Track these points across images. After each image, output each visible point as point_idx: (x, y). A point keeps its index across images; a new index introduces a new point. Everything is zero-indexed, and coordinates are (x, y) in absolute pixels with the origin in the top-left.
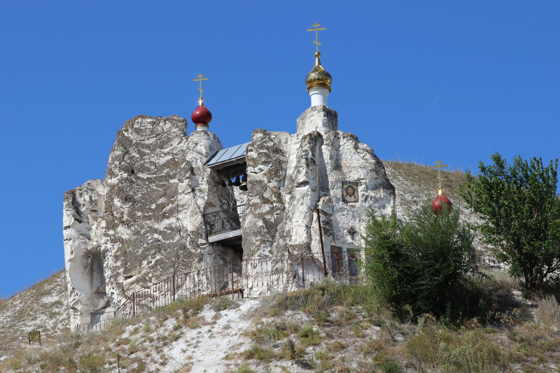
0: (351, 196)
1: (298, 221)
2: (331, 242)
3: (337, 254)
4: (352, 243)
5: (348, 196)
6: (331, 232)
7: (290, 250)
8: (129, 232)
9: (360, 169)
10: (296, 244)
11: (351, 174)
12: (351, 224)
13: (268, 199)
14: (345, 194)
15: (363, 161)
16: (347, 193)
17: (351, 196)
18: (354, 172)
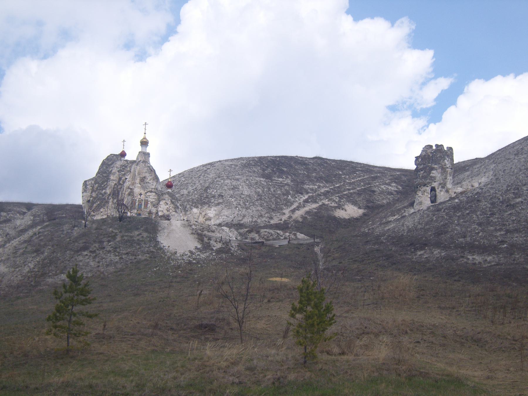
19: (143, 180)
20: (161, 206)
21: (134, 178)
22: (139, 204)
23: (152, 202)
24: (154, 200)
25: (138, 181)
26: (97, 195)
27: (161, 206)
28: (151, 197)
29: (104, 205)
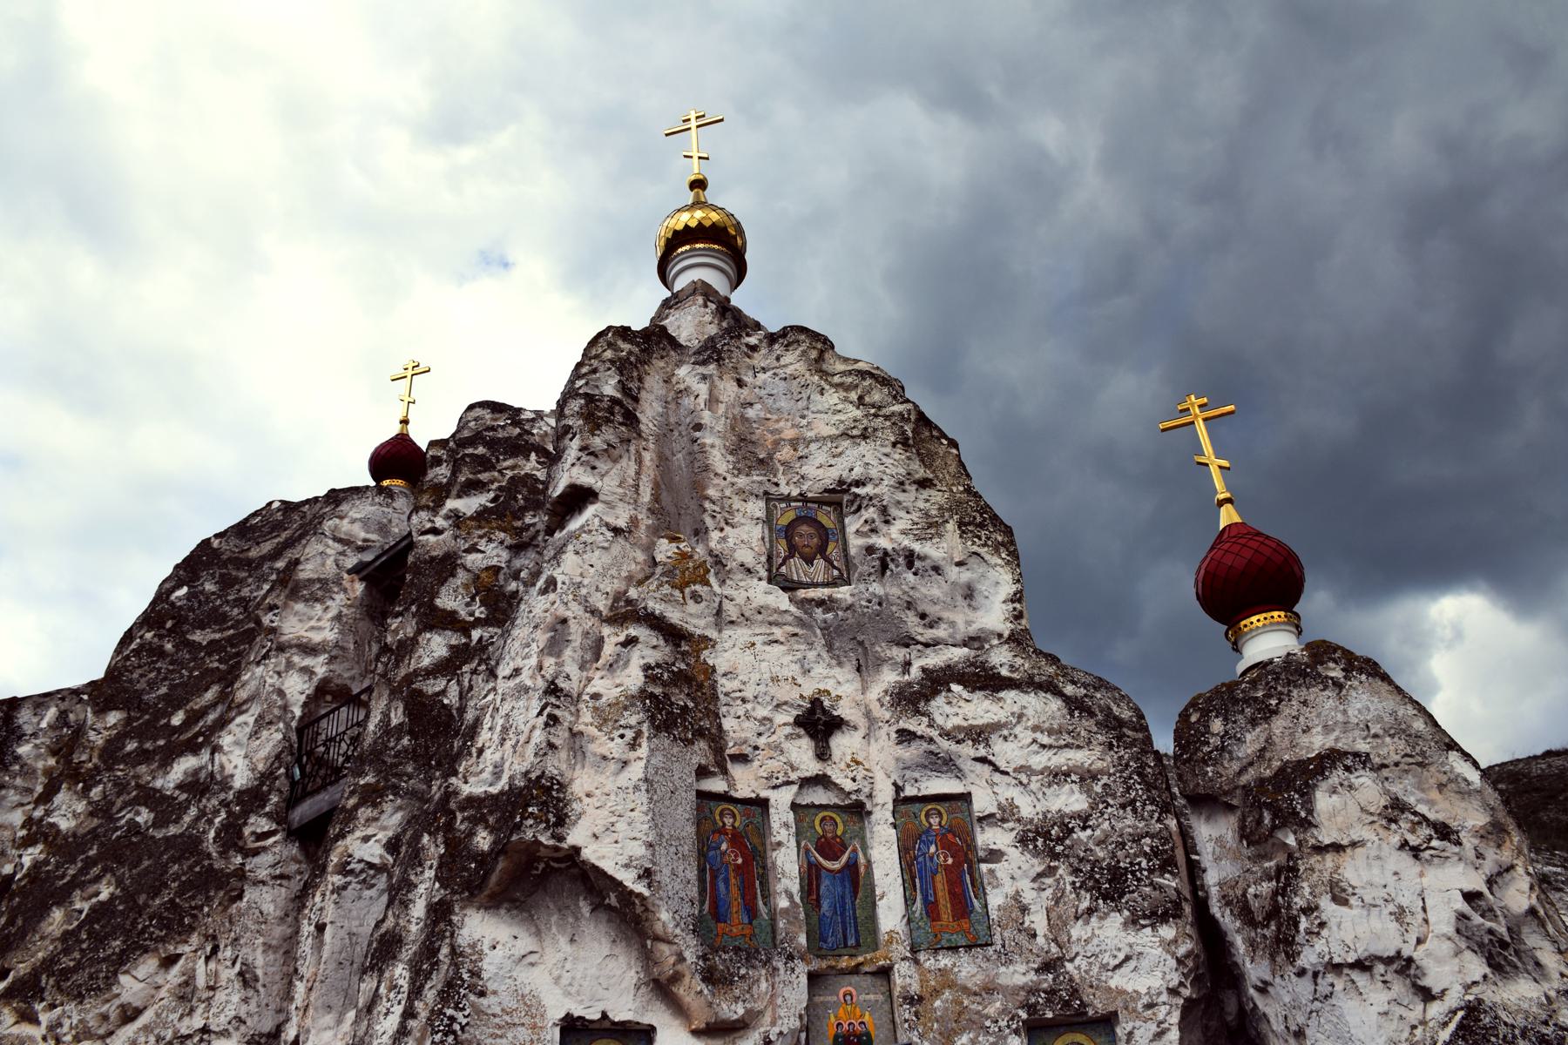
0: (809, 562)
1: (517, 672)
2: (702, 772)
3: (737, 839)
4: (822, 781)
5: (796, 561)
6: (706, 723)
7: (461, 826)
8: (81, 807)
9: (847, 443)
10: (494, 790)
11: (809, 469)
12: (809, 689)
13: (454, 613)
14: (782, 548)
15: (858, 413)
16: (792, 550)
17: (809, 562)
18: (819, 455)
19: (810, 530)
20: (1353, 870)
21: (678, 507)
22: (811, 876)
23: (1046, 838)
24: (1071, 800)
25: (744, 538)
26: (102, 810)
27: (1353, 870)
28: (1007, 752)
29: (177, 923)
